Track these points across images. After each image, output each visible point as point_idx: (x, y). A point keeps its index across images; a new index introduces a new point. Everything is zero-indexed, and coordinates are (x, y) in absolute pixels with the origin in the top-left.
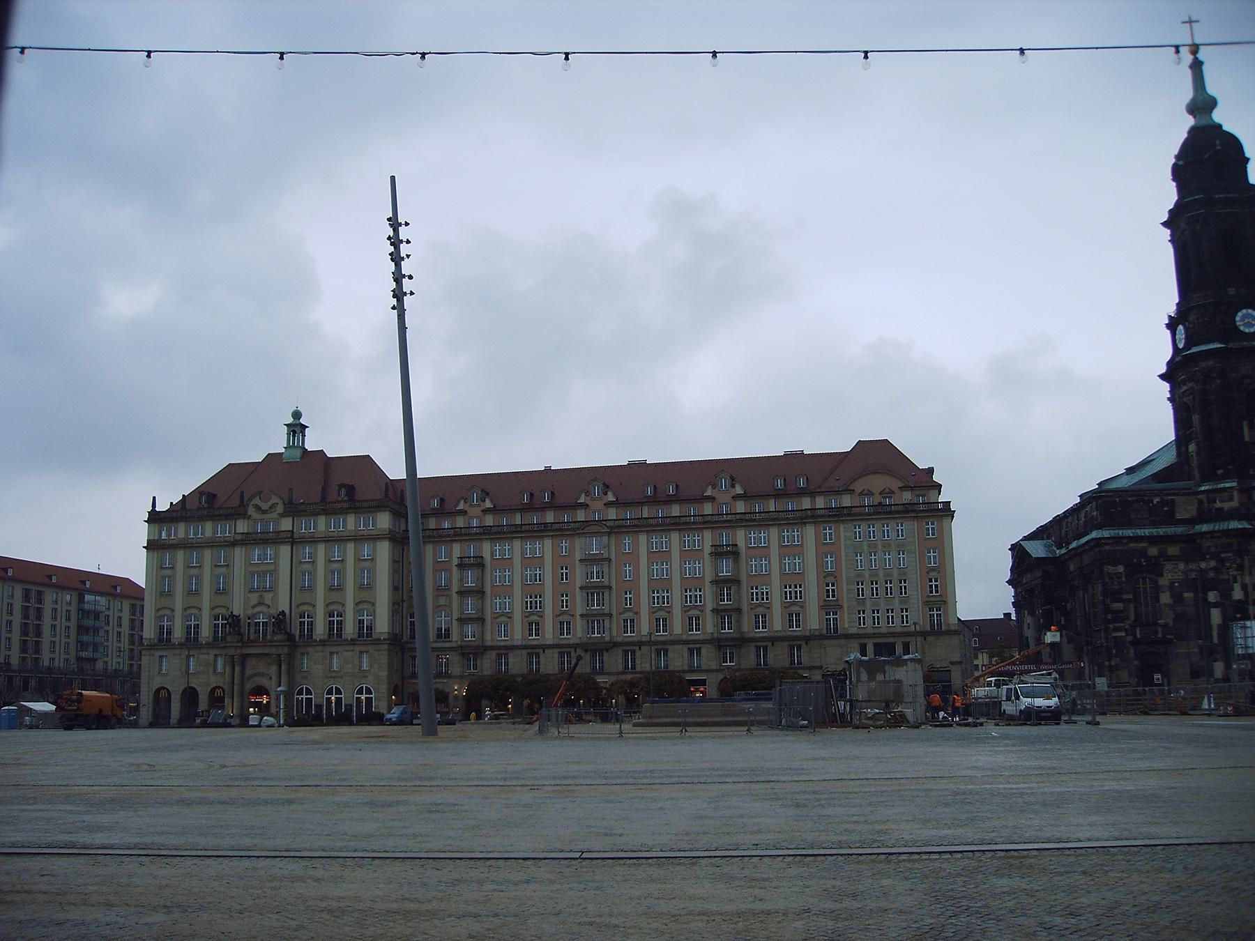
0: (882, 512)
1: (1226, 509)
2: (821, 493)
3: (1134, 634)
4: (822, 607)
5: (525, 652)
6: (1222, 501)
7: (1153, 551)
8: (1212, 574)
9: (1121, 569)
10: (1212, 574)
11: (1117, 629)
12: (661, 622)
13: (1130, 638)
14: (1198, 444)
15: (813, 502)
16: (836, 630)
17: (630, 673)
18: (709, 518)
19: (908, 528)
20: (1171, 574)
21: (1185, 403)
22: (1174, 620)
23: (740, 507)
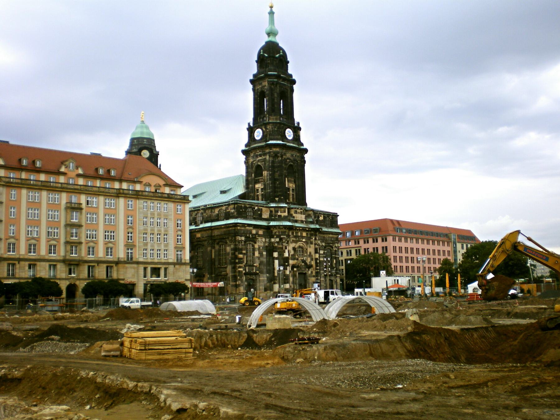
3: (246, 270)
6: (281, 212)
7: (254, 232)
8: (276, 245)
9: (243, 238)
10: (276, 245)
11: (240, 267)
13: (244, 272)
14: (265, 185)
20: (261, 242)
21: (259, 165)
22: (259, 264)
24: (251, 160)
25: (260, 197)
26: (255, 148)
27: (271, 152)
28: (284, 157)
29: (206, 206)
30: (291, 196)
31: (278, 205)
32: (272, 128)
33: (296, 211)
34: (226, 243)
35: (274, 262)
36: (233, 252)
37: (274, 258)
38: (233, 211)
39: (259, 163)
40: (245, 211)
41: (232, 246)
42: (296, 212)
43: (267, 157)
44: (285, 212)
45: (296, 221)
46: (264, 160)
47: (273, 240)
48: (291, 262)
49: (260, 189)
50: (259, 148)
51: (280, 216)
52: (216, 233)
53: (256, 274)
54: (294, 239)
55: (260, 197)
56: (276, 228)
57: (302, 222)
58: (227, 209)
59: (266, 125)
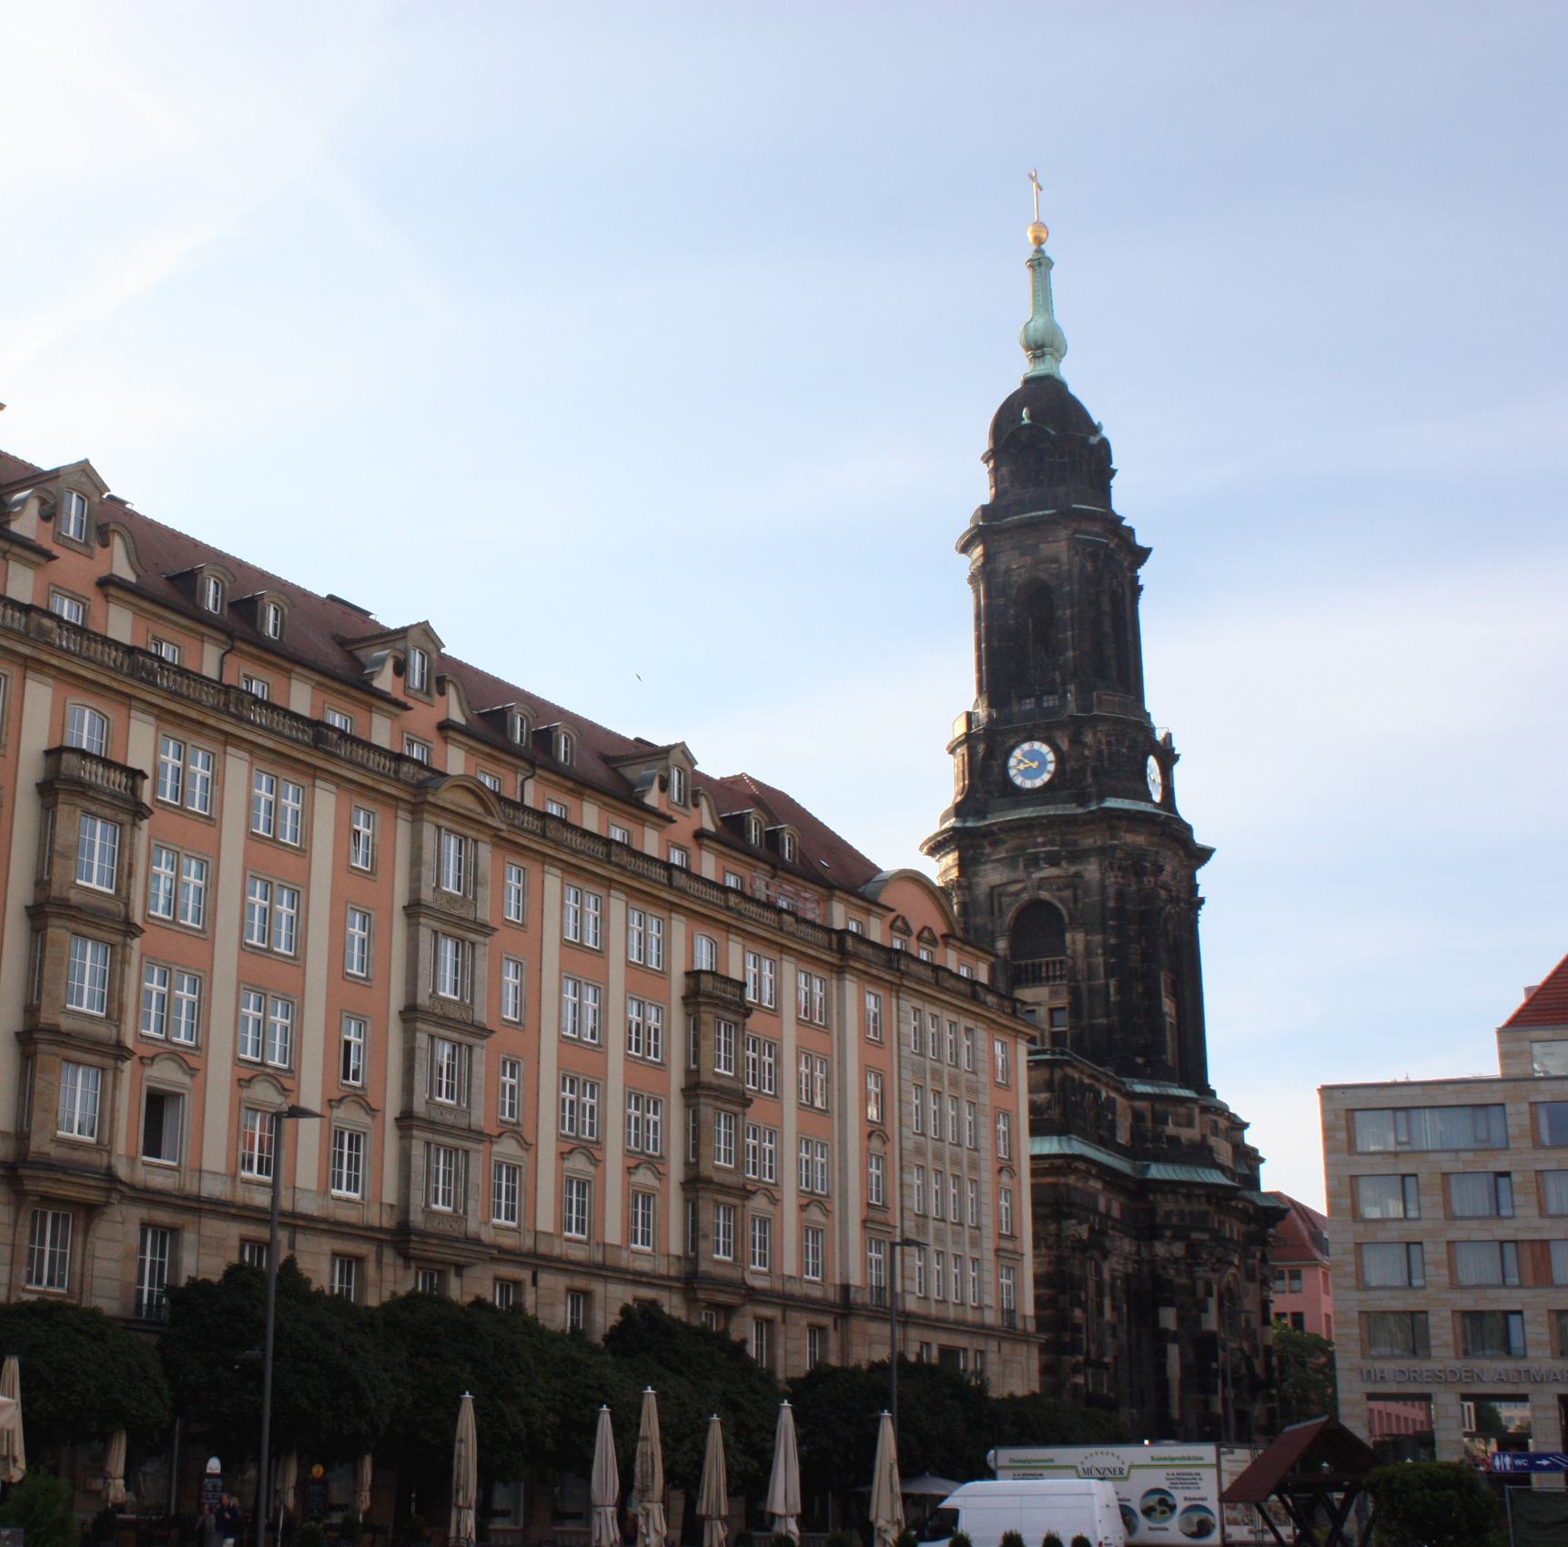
6: (1177, 1124)
14: (1074, 993)
27: (1114, 848)
32: (1109, 743)
33: (1216, 1123)
35: (1162, 1354)
37: (1162, 1337)
39: (1044, 895)
43: (1092, 870)
44: (1190, 1123)
46: (1075, 882)
47: (1160, 1249)
50: (1052, 822)
51: (1174, 1140)
56: (1175, 1193)
59: (1076, 727)
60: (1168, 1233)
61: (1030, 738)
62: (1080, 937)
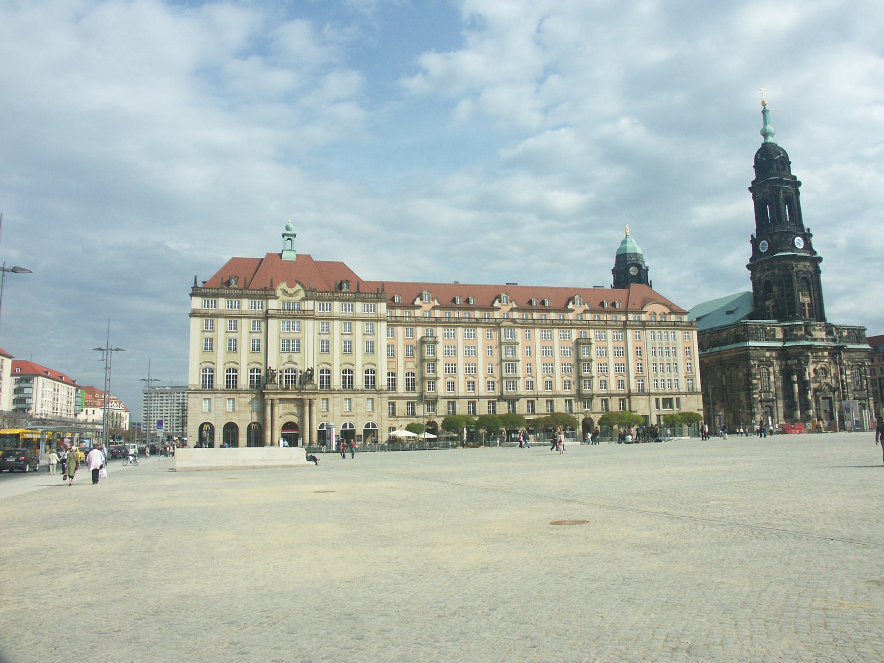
0: (661, 325)
1: (799, 335)
2: (632, 312)
3: (761, 396)
4: (635, 378)
5: (466, 401)
8: (794, 367)
10: (794, 367)
11: (755, 394)
12: (549, 385)
13: (759, 398)
14: (776, 302)
15: (627, 317)
16: (643, 390)
17: (530, 414)
18: (573, 322)
19: (679, 334)
23: (589, 316)
24: (758, 275)
25: (772, 315)
26: (761, 262)
28: (795, 269)
29: (712, 329)
30: (807, 312)
31: (793, 323)
34: (738, 368)
36: (746, 377)
38: (743, 333)
39: (768, 278)
40: (756, 333)
41: (745, 371)
42: (814, 330)
43: (777, 271)
44: (801, 330)
45: (815, 340)
47: (789, 362)
48: (813, 386)
49: (770, 307)
52: (725, 356)
53: (772, 401)
54: (815, 360)
55: (772, 315)
57: (822, 340)
58: (736, 331)
60: (792, 358)
61: (763, 240)
62: (776, 287)
